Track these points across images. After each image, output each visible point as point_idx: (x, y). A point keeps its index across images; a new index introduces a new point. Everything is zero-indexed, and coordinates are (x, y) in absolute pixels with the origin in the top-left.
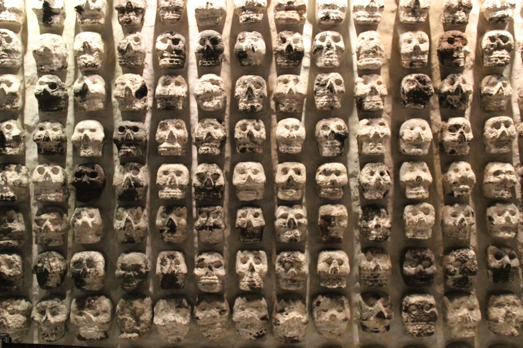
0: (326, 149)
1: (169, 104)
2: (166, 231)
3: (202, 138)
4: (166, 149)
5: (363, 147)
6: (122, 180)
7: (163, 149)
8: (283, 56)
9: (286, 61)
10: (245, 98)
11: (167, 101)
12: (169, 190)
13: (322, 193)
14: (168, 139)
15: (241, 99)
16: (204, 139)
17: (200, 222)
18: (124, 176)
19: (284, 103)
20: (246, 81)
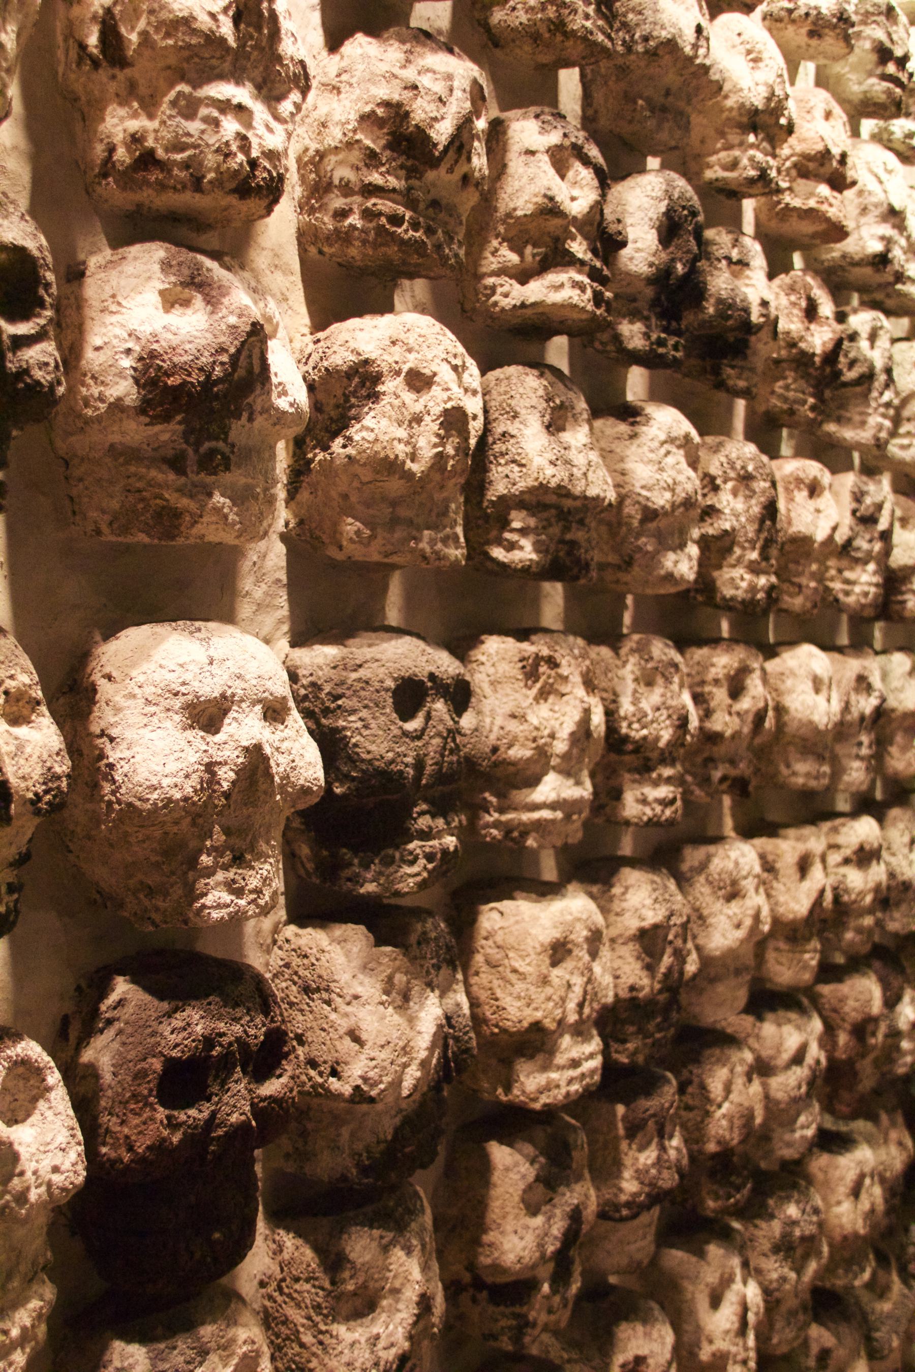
0: (856, 764)
1: (573, 544)
2: (546, 1288)
3: (658, 739)
4: (559, 815)
5: (894, 750)
6: (406, 1050)
7: (546, 814)
8: (806, 376)
9: (811, 400)
10: (754, 548)
11: (567, 529)
12: (575, 1053)
13: (849, 935)
14: (566, 757)
15: (738, 551)
16: (662, 744)
17: (640, 1175)
18: (411, 1021)
19: (804, 581)
20: (750, 468)
